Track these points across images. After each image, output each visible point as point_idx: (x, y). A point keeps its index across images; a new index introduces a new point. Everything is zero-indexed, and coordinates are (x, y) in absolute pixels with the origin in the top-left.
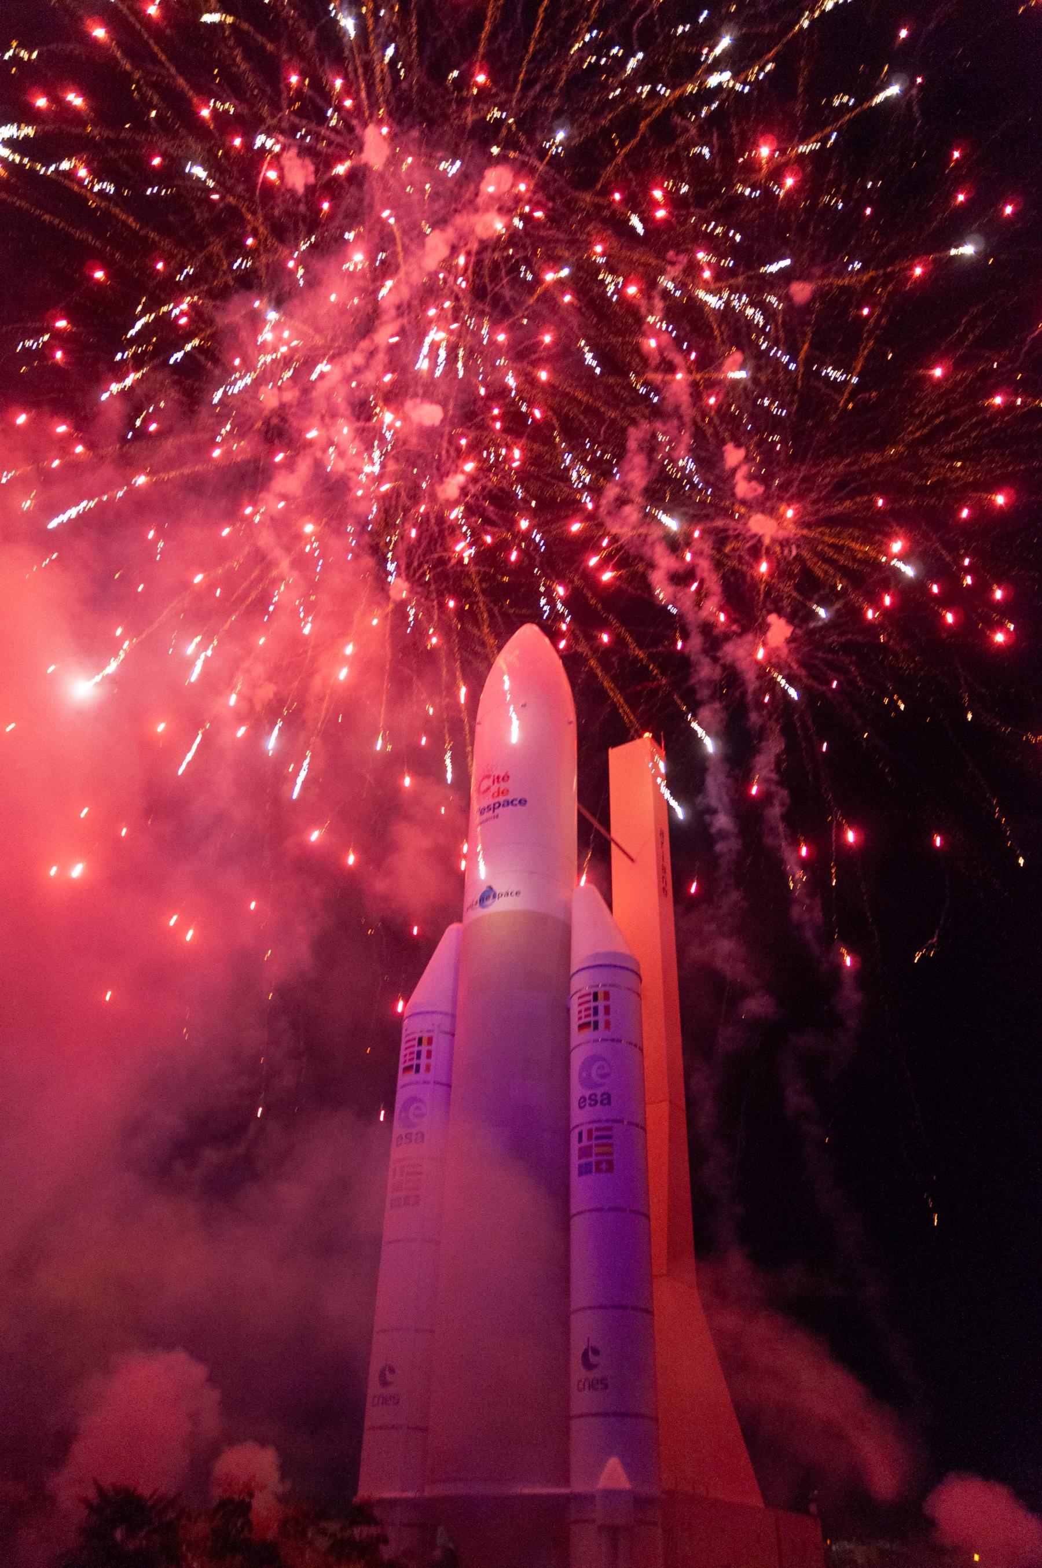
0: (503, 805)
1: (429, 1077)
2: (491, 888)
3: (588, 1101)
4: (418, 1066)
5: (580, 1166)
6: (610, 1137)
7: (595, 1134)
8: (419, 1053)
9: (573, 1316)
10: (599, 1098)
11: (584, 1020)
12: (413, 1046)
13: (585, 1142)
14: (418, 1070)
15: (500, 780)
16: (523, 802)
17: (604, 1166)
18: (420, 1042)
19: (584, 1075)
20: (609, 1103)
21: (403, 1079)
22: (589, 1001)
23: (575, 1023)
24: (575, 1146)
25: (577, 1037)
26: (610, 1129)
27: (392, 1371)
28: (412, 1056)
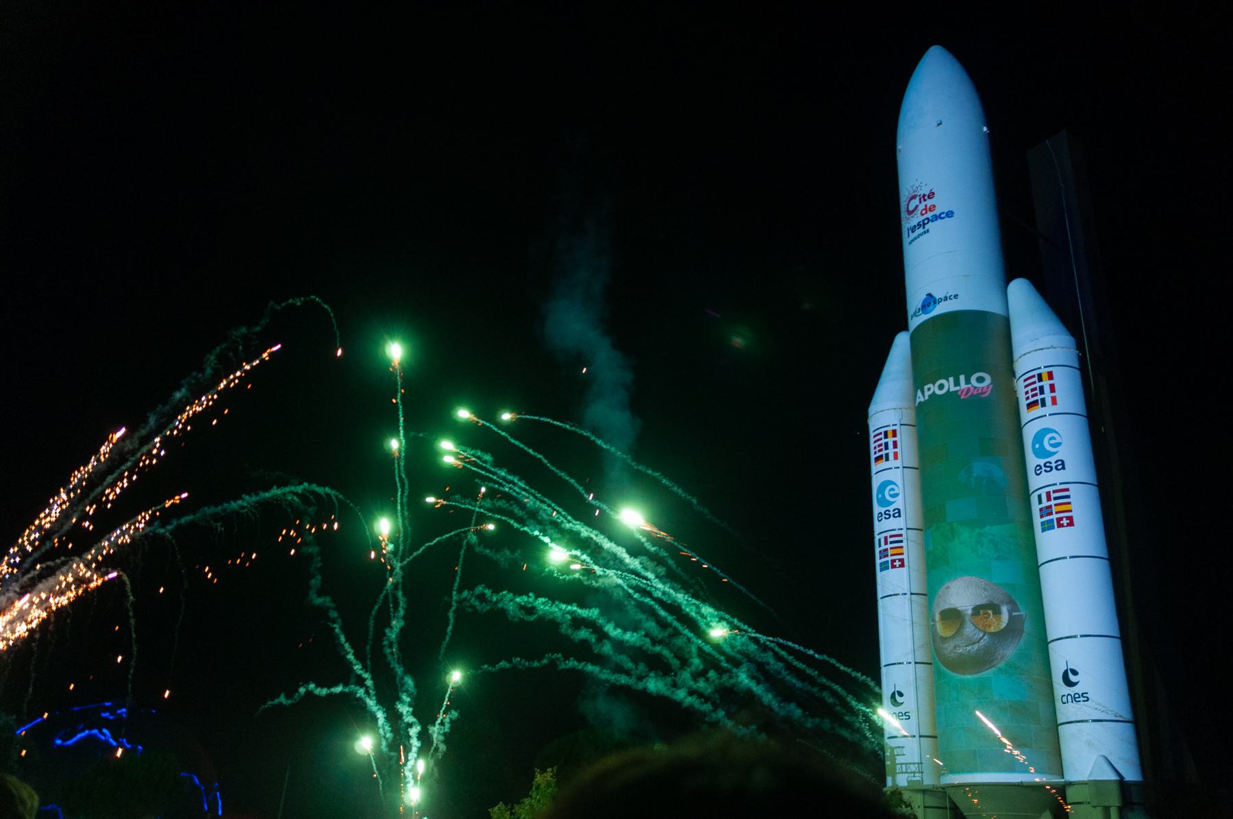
0: (932, 221)
1: (898, 463)
2: (930, 295)
3: (1044, 468)
4: (887, 455)
5: (1043, 524)
6: (1068, 497)
7: (1053, 495)
8: (886, 444)
9: (1049, 645)
10: (1053, 465)
11: (1031, 400)
12: (881, 439)
13: (1045, 503)
14: (887, 459)
15: (926, 197)
16: (950, 214)
17: (1065, 522)
18: (886, 436)
19: (1037, 446)
20: (1063, 468)
21: (875, 467)
22: (1034, 383)
23: (1023, 403)
24: (1036, 507)
25: (1026, 415)
26: (1067, 490)
27: (901, 694)
28: (880, 448)
